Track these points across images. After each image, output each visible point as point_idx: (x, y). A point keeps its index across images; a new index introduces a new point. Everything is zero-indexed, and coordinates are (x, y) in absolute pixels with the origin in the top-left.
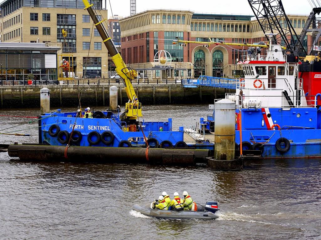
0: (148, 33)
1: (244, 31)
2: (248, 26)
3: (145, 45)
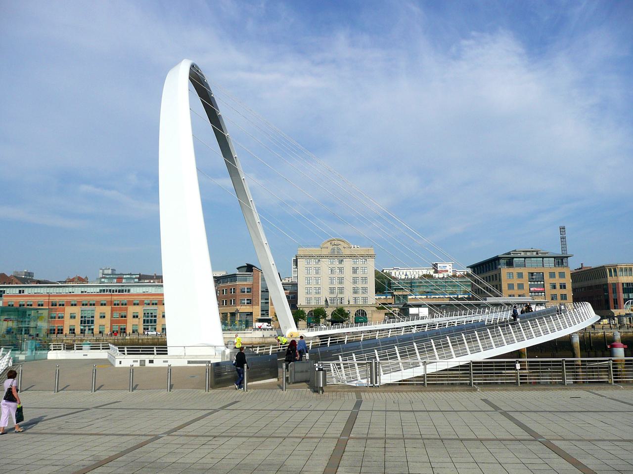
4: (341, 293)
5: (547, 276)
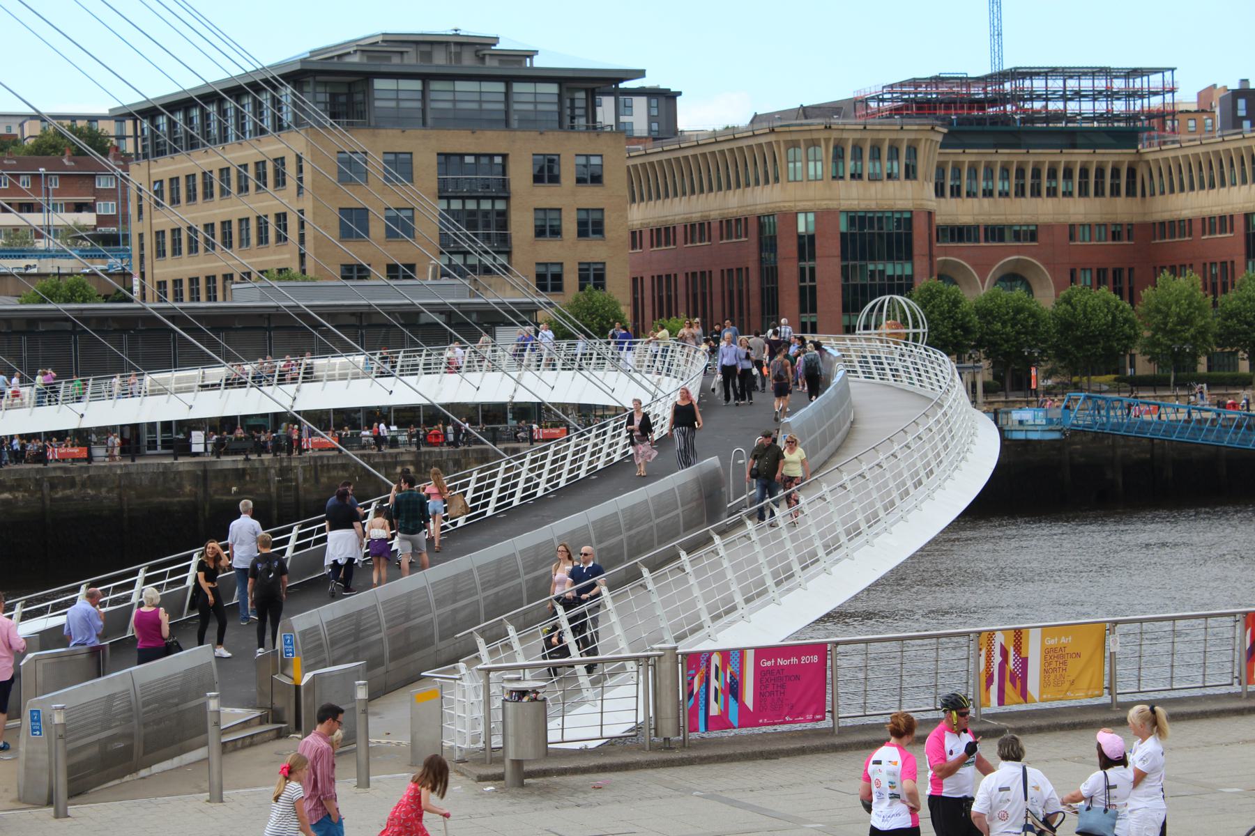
1: (1115, 192)
2: (1132, 172)
3: (753, 265)
5: (520, 175)
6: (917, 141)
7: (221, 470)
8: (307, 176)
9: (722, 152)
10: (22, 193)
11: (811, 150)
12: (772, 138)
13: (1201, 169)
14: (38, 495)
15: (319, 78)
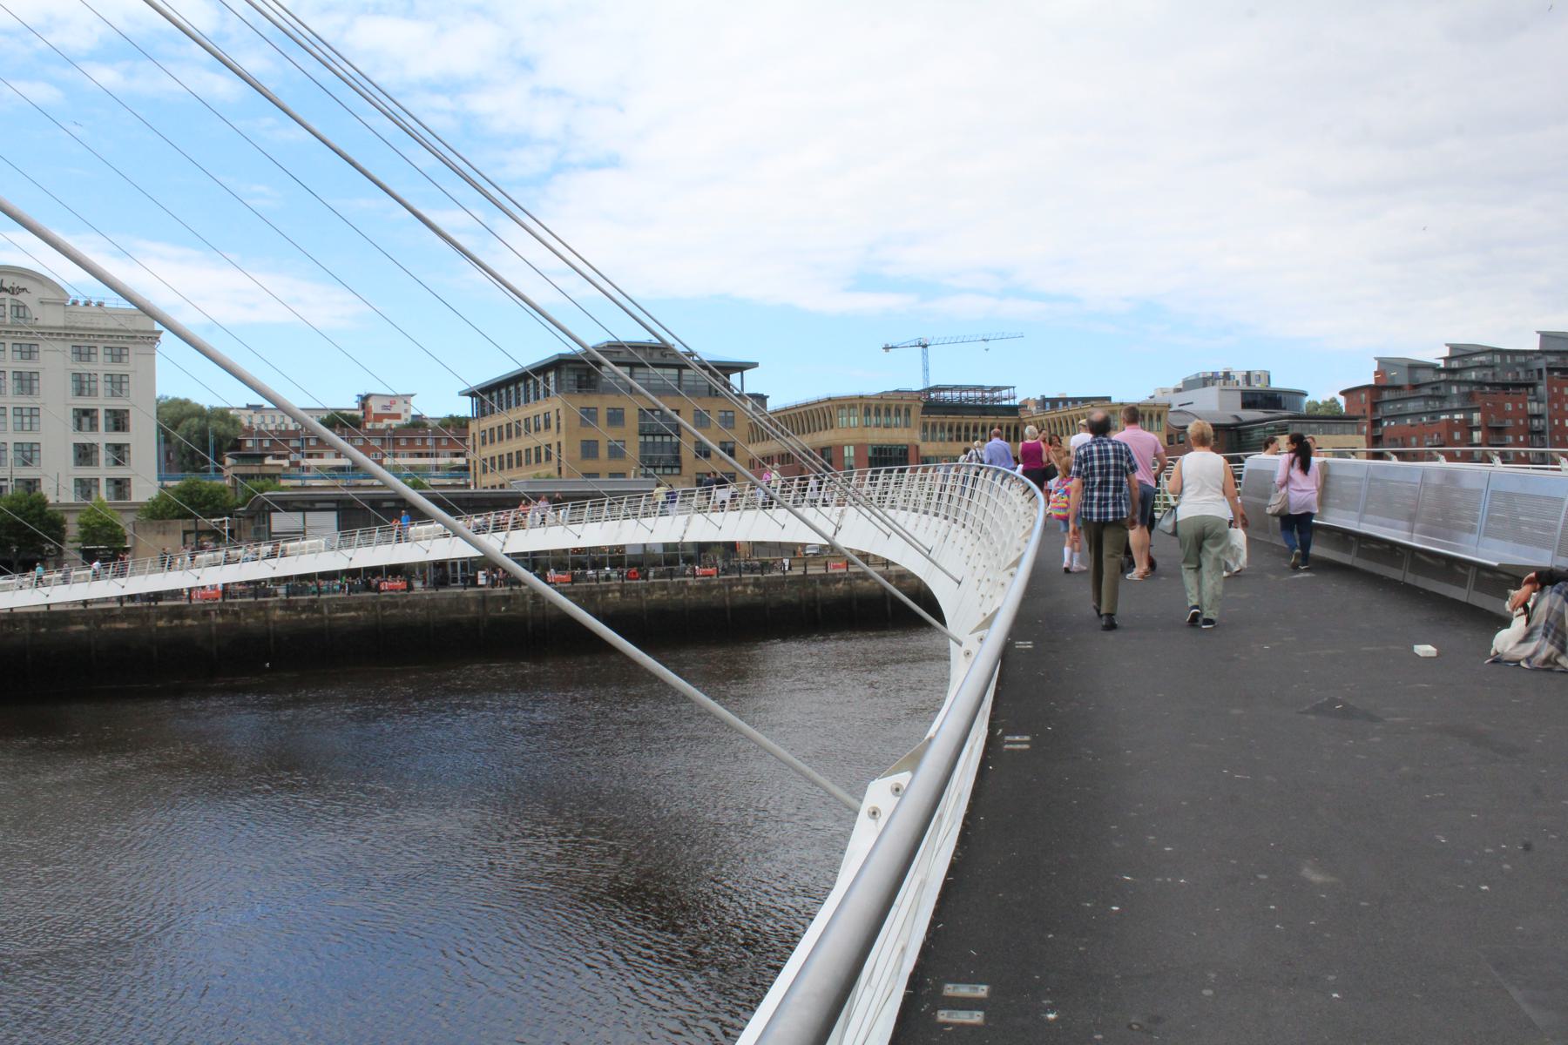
0: (829, 448)
2: (1016, 429)
4: (27, 462)
6: (911, 406)
7: (494, 597)
8: (562, 422)
9: (800, 413)
10: (428, 447)
11: (851, 411)
12: (829, 404)
13: (1055, 426)
14: (374, 613)
15: (570, 365)
